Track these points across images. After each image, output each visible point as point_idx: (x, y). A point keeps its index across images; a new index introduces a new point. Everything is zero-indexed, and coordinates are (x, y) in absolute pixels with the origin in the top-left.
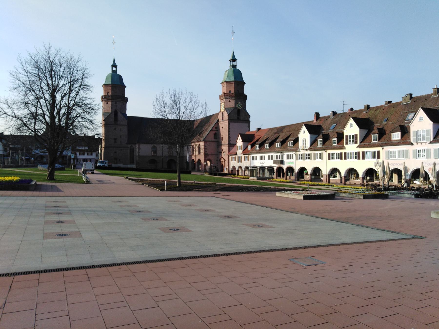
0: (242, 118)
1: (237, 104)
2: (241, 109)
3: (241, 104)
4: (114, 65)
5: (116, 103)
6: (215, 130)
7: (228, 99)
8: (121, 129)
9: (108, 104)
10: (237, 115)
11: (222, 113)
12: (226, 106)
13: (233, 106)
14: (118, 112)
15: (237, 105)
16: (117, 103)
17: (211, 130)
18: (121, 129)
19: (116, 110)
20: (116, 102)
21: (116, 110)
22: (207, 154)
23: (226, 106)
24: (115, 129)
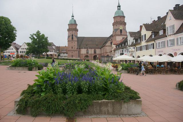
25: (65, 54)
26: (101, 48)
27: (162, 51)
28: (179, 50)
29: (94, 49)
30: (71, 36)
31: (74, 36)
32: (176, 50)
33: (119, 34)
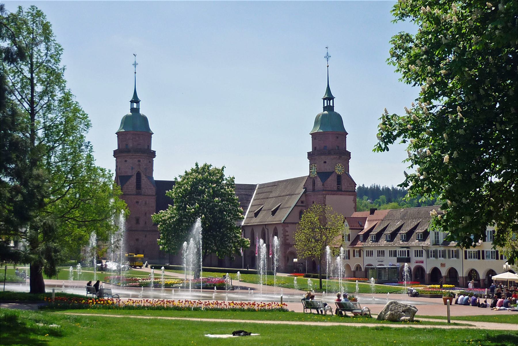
0: (344, 187)
1: (337, 166)
3: (342, 166)
5: (139, 161)
6: (301, 206)
8: (146, 202)
9: (126, 163)
10: (336, 184)
11: (312, 179)
14: (142, 175)
17: (295, 206)
18: (146, 202)
20: (140, 159)
22: (289, 243)
24: (137, 202)
30: (133, 180)
33: (333, 189)
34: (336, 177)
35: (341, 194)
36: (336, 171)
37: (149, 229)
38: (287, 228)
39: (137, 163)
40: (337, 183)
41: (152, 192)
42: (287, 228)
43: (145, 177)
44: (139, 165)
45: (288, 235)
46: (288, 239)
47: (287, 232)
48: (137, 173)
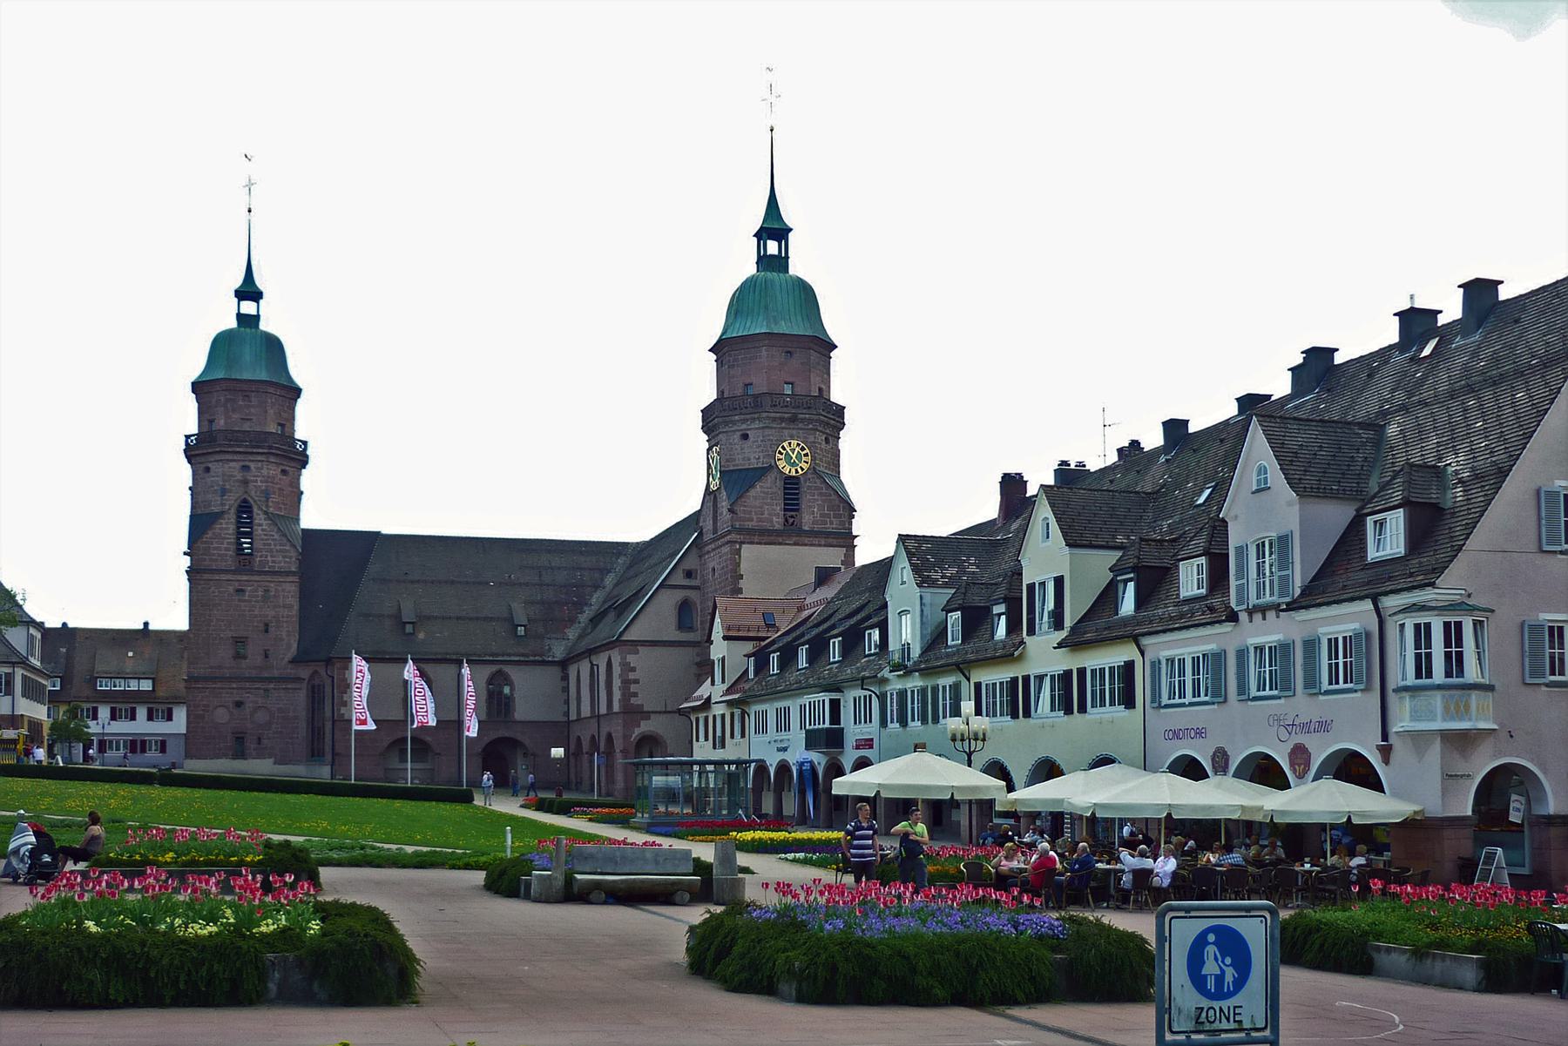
0: (807, 520)
2: (800, 472)
4: (249, 291)
5: (246, 468)
7: (734, 423)
8: (267, 591)
9: (207, 475)
12: (727, 461)
13: (759, 458)
14: (255, 510)
15: (780, 453)
16: (252, 465)
18: (267, 591)
19: (245, 501)
20: (247, 463)
21: (245, 501)
23: (727, 461)
24: (240, 591)
25: (142, 712)
26: (564, 664)
27: (1200, 733)
28: (1324, 726)
29: (487, 671)
31: (259, 517)
32: (1306, 728)
33: (767, 525)
34: (780, 484)
35: (795, 544)
36: (781, 464)
37: (276, 673)
38: (631, 658)
39: (239, 476)
40: (785, 504)
41: (285, 562)
42: (631, 658)
43: (262, 516)
44: (245, 482)
45: (636, 681)
46: (635, 695)
47: (633, 670)
48: (240, 506)
